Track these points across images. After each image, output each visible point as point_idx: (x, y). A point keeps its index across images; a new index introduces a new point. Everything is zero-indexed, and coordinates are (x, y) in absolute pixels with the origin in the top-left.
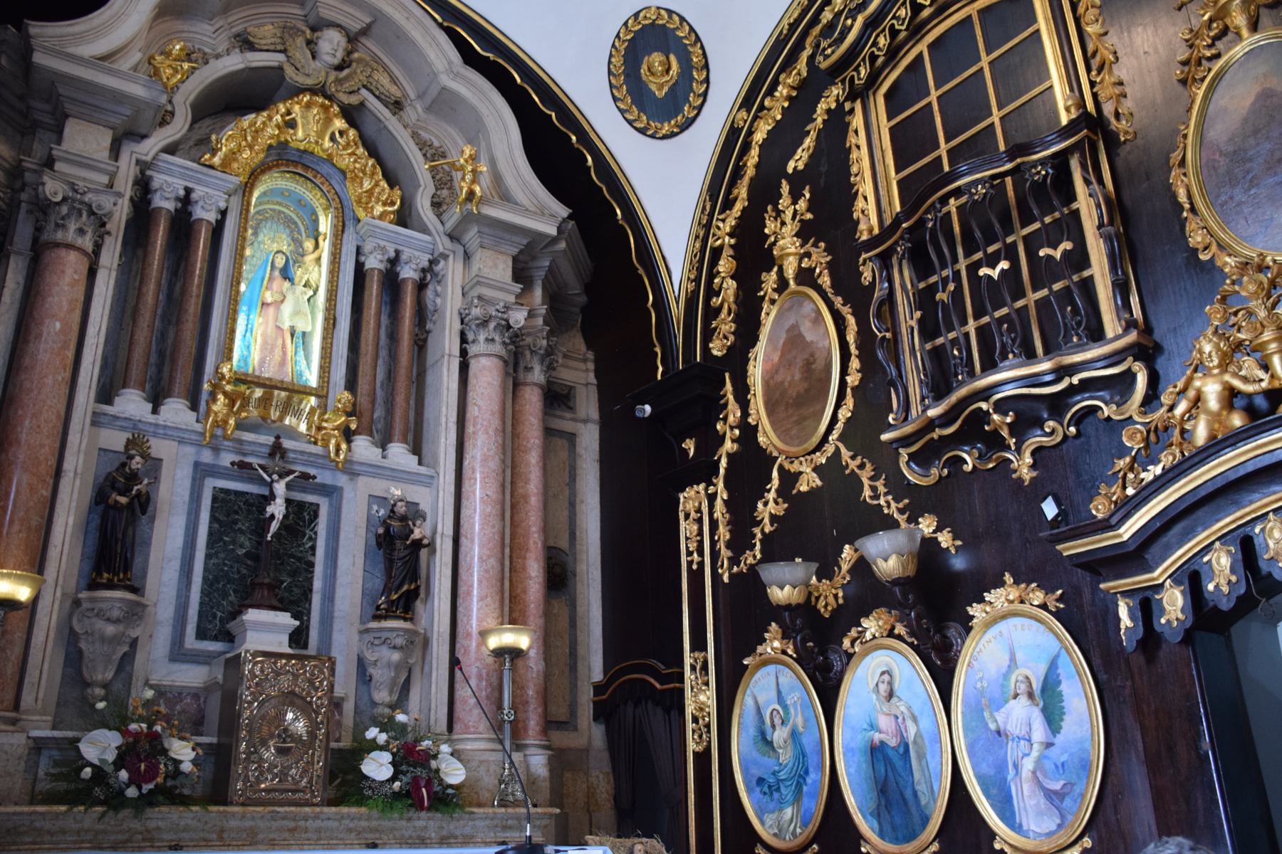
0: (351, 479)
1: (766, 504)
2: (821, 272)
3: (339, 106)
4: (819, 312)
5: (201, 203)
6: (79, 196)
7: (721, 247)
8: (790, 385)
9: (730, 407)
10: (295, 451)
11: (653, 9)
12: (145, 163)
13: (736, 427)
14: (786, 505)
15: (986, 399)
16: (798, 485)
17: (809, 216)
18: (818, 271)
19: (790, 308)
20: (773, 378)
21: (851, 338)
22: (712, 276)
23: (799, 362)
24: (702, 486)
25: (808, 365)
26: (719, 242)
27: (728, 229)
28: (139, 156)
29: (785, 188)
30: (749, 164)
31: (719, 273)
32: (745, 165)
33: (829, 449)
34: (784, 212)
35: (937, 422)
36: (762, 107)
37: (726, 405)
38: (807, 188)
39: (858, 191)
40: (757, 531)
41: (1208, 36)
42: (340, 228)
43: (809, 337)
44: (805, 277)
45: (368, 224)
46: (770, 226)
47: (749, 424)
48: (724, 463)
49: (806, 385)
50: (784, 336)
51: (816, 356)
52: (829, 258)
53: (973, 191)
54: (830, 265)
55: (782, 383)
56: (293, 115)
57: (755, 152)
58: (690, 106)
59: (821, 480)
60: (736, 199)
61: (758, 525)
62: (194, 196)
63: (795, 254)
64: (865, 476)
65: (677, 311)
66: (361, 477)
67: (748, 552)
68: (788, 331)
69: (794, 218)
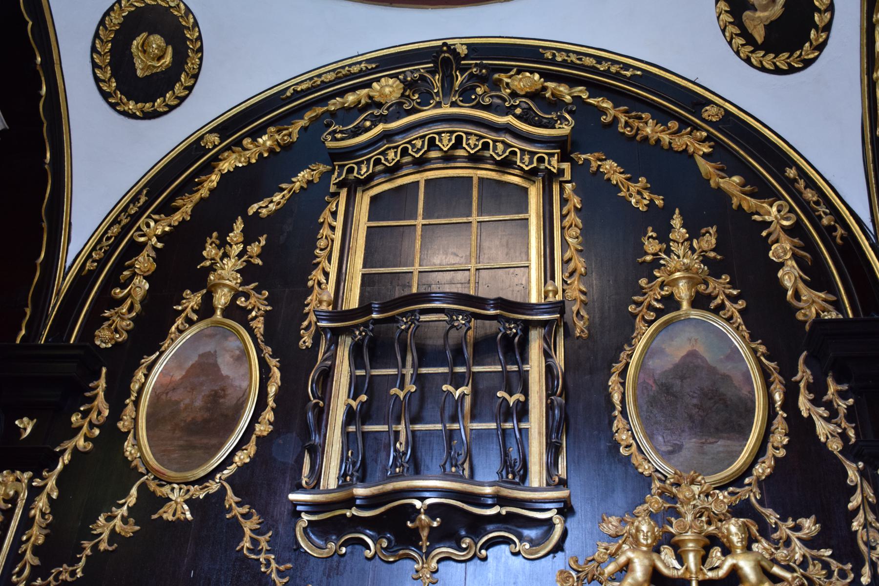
1: (110, 519)
2: (256, 317)
4: (245, 353)
7: (143, 245)
8: (186, 408)
9: (96, 403)
13: (98, 426)
14: (137, 528)
15: (422, 499)
16: (161, 511)
17: (258, 261)
18: (254, 314)
19: (211, 336)
20: (167, 393)
21: (272, 390)
22: (119, 266)
23: (206, 390)
24: (27, 475)
25: (215, 397)
26: (142, 239)
27: (159, 232)
29: (239, 225)
30: (205, 185)
31: (132, 266)
32: (201, 183)
33: (213, 487)
34: (231, 246)
35: (358, 502)
36: (238, 143)
37: (93, 398)
38: (265, 236)
39: (319, 263)
40: (88, 545)
41: (659, 293)
43: (225, 371)
44: (233, 311)
46: (210, 251)
47: (119, 429)
48: (67, 457)
49: (206, 415)
50: (194, 359)
51: (229, 391)
52: (269, 308)
53: (455, 318)
54: (267, 315)
55: (177, 403)
57: (215, 178)
58: (164, 101)
59: (192, 514)
60: (178, 209)
61: (91, 540)
63: (231, 288)
64: (248, 526)
65: (63, 283)
67: (65, 566)
68: (201, 356)
69: (240, 255)
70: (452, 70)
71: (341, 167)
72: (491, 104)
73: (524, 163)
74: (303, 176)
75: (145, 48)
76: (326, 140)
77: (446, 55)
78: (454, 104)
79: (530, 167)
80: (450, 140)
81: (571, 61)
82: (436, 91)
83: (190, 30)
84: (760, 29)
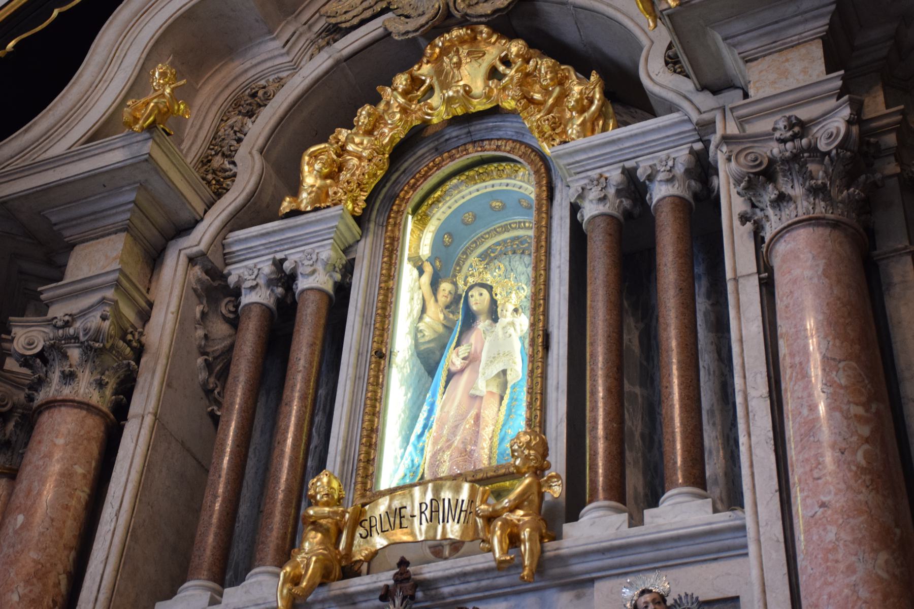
0: (578, 597)
3: (487, 24)
5: (300, 270)
6: (61, 332)
10: (448, 579)
12: (203, 254)
28: (188, 251)
42: (544, 195)
45: (559, 157)
56: (428, 81)
62: (287, 266)
66: (598, 585)
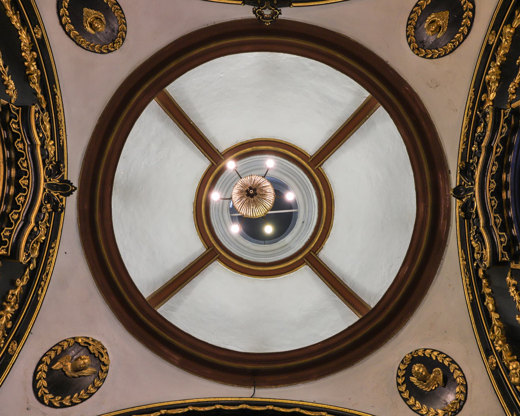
11: (118, 49)
30: (15, 17)
58: (66, 15)
70: (60, 190)
71: (17, 111)
72: (42, 212)
73: (5, 232)
74: (11, 84)
75: (99, 19)
76: (36, 107)
77: (71, 189)
78: (44, 189)
79: (3, 236)
80: (24, 185)
81: (49, 258)
82: (51, 179)
83: (100, 48)
84: (60, 367)
